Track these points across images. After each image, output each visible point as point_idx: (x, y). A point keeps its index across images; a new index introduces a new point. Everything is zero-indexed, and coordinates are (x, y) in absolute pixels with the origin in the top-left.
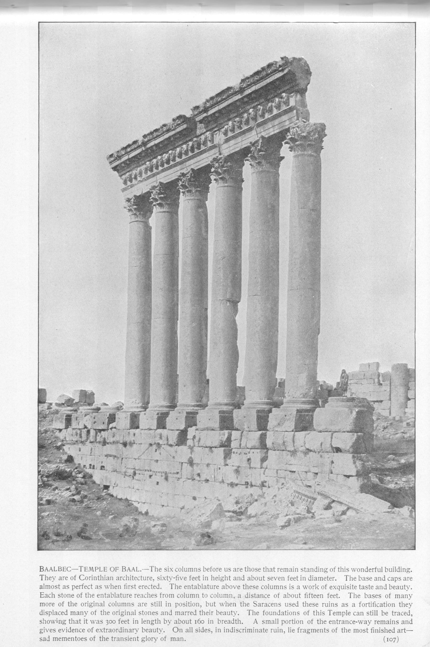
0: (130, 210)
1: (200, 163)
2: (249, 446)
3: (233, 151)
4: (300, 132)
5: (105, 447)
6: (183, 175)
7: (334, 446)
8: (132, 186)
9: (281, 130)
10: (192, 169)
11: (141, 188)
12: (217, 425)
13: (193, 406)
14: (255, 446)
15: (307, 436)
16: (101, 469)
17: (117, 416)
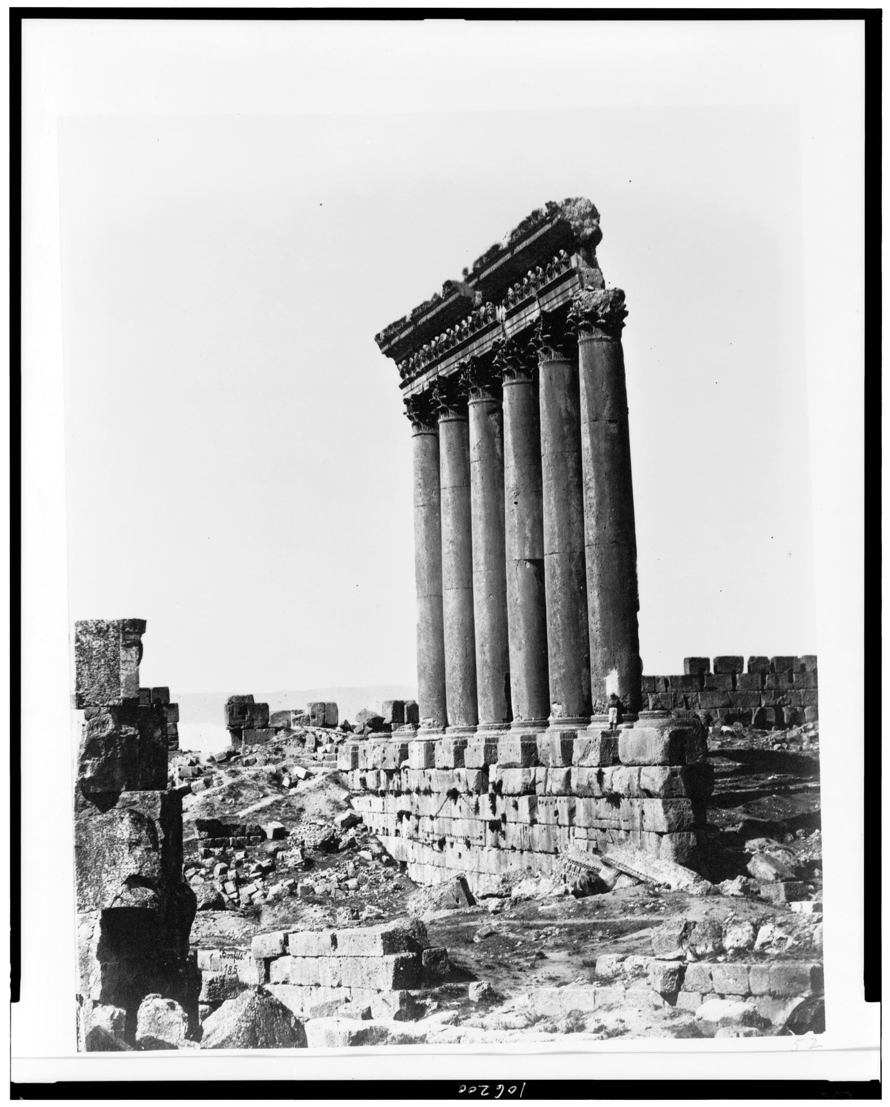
0: (410, 418)
1: (485, 346)
2: (554, 791)
3: (518, 331)
4: (583, 307)
5: (399, 798)
6: (463, 366)
7: (642, 787)
8: (411, 380)
9: (566, 301)
10: (473, 358)
11: (422, 384)
12: (518, 759)
13: (499, 729)
14: (560, 791)
15: (616, 773)
16: (396, 835)
17: (409, 748)
